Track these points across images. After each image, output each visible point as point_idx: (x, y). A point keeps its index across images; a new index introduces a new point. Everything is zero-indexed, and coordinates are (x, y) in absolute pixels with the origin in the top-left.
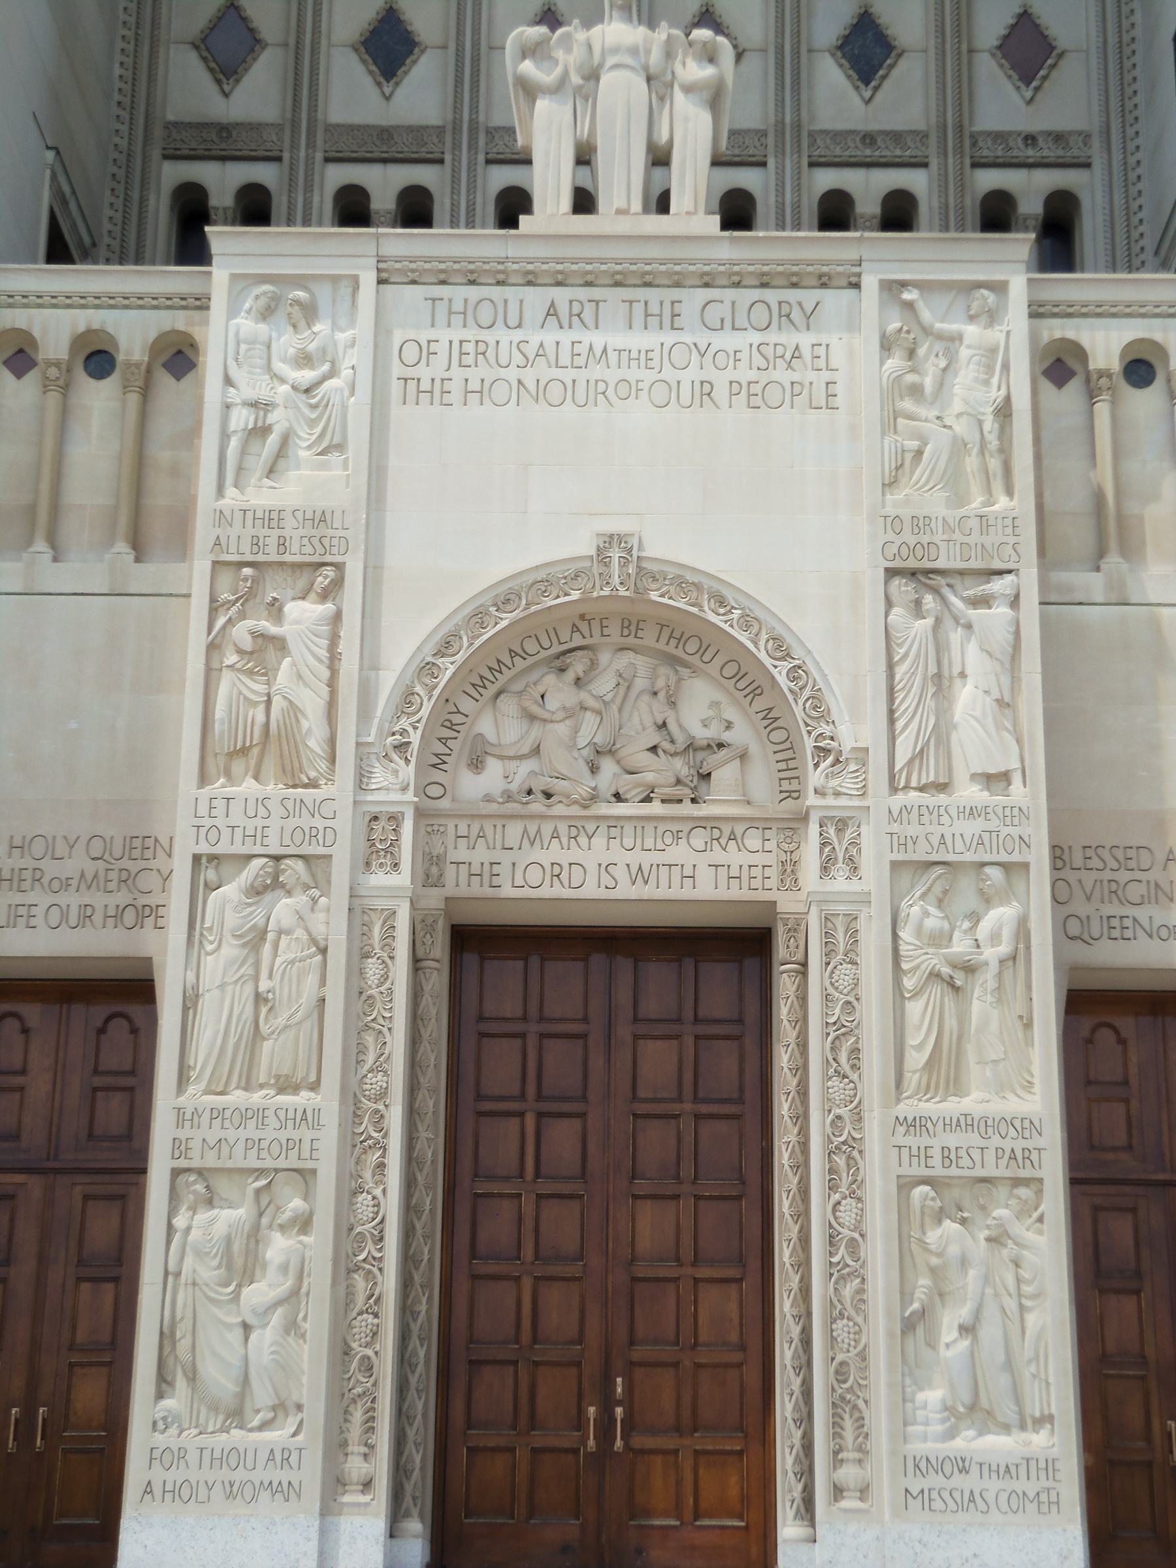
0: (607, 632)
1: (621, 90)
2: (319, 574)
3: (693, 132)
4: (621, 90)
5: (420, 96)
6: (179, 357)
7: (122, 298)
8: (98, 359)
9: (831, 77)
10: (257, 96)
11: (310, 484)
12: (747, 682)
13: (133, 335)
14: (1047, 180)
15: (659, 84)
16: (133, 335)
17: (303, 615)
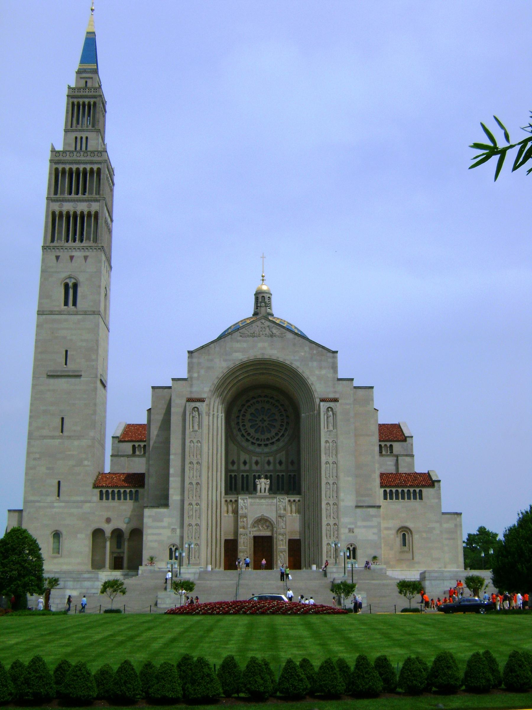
0: (262, 521)
1: (263, 484)
2: (246, 517)
3: (268, 487)
4: (263, 484)
5: (247, 467)
6: (237, 501)
7: (233, 498)
8: (231, 501)
9: (278, 465)
10: (235, 467)
11: (245, 511)
12: (270, 522)
13: (233, 500)
14: (293, 474)
15: (265, 484)
16: (233, 500)
17: (245, 519)
